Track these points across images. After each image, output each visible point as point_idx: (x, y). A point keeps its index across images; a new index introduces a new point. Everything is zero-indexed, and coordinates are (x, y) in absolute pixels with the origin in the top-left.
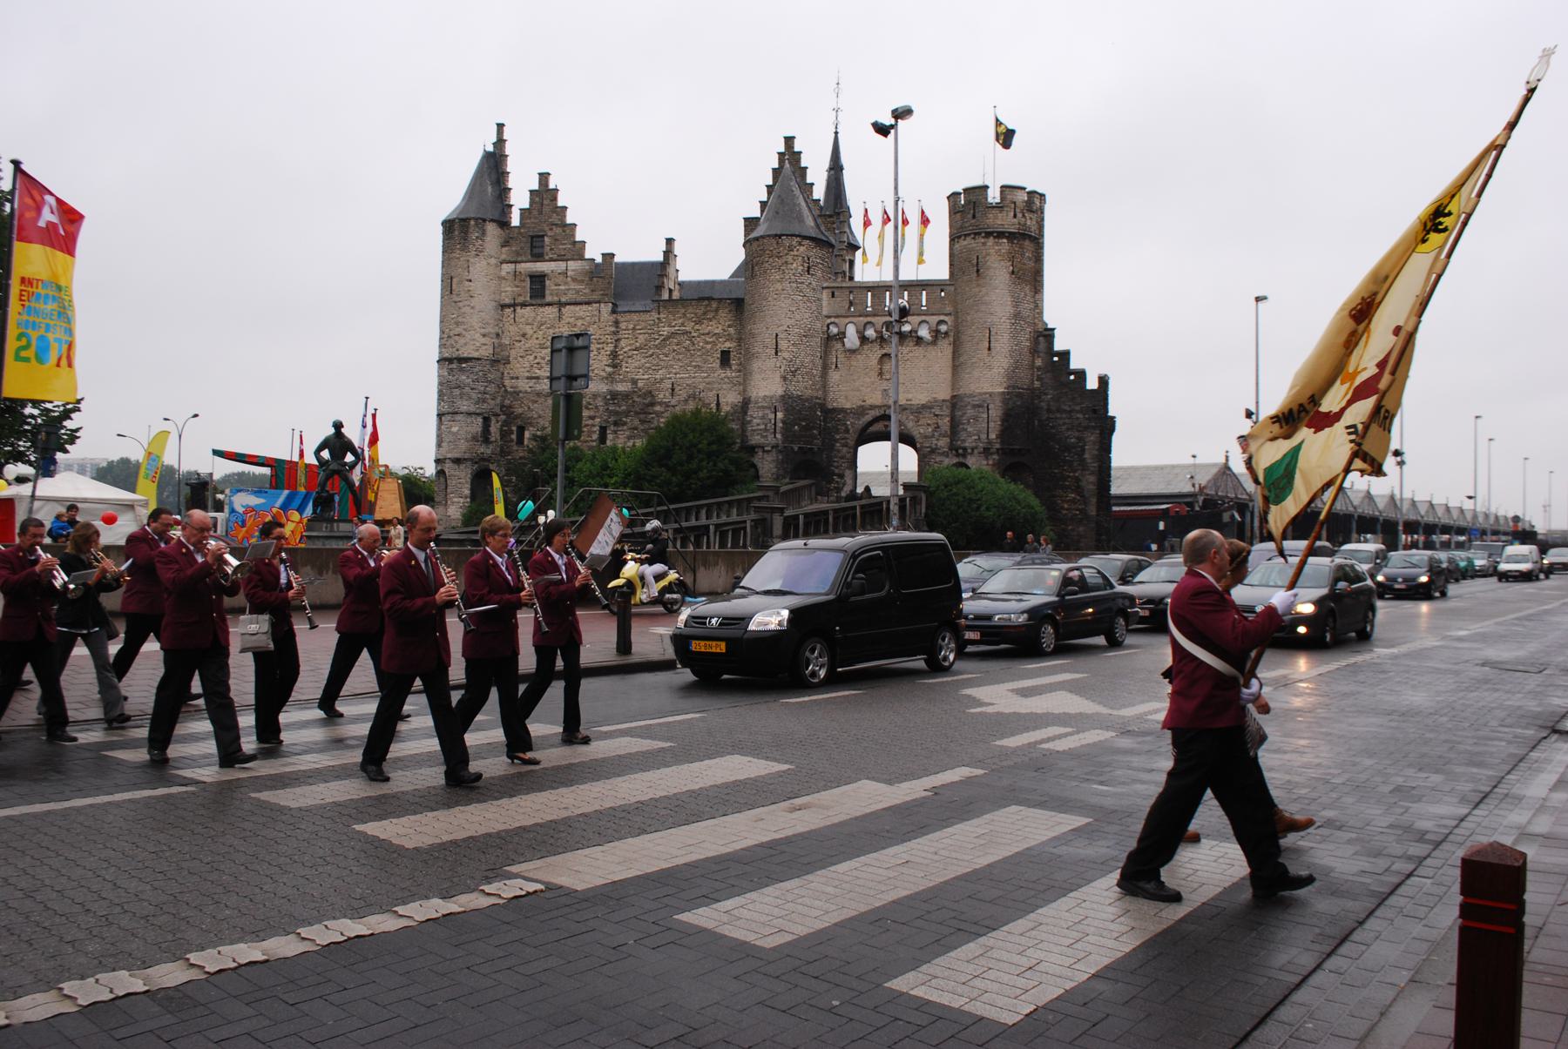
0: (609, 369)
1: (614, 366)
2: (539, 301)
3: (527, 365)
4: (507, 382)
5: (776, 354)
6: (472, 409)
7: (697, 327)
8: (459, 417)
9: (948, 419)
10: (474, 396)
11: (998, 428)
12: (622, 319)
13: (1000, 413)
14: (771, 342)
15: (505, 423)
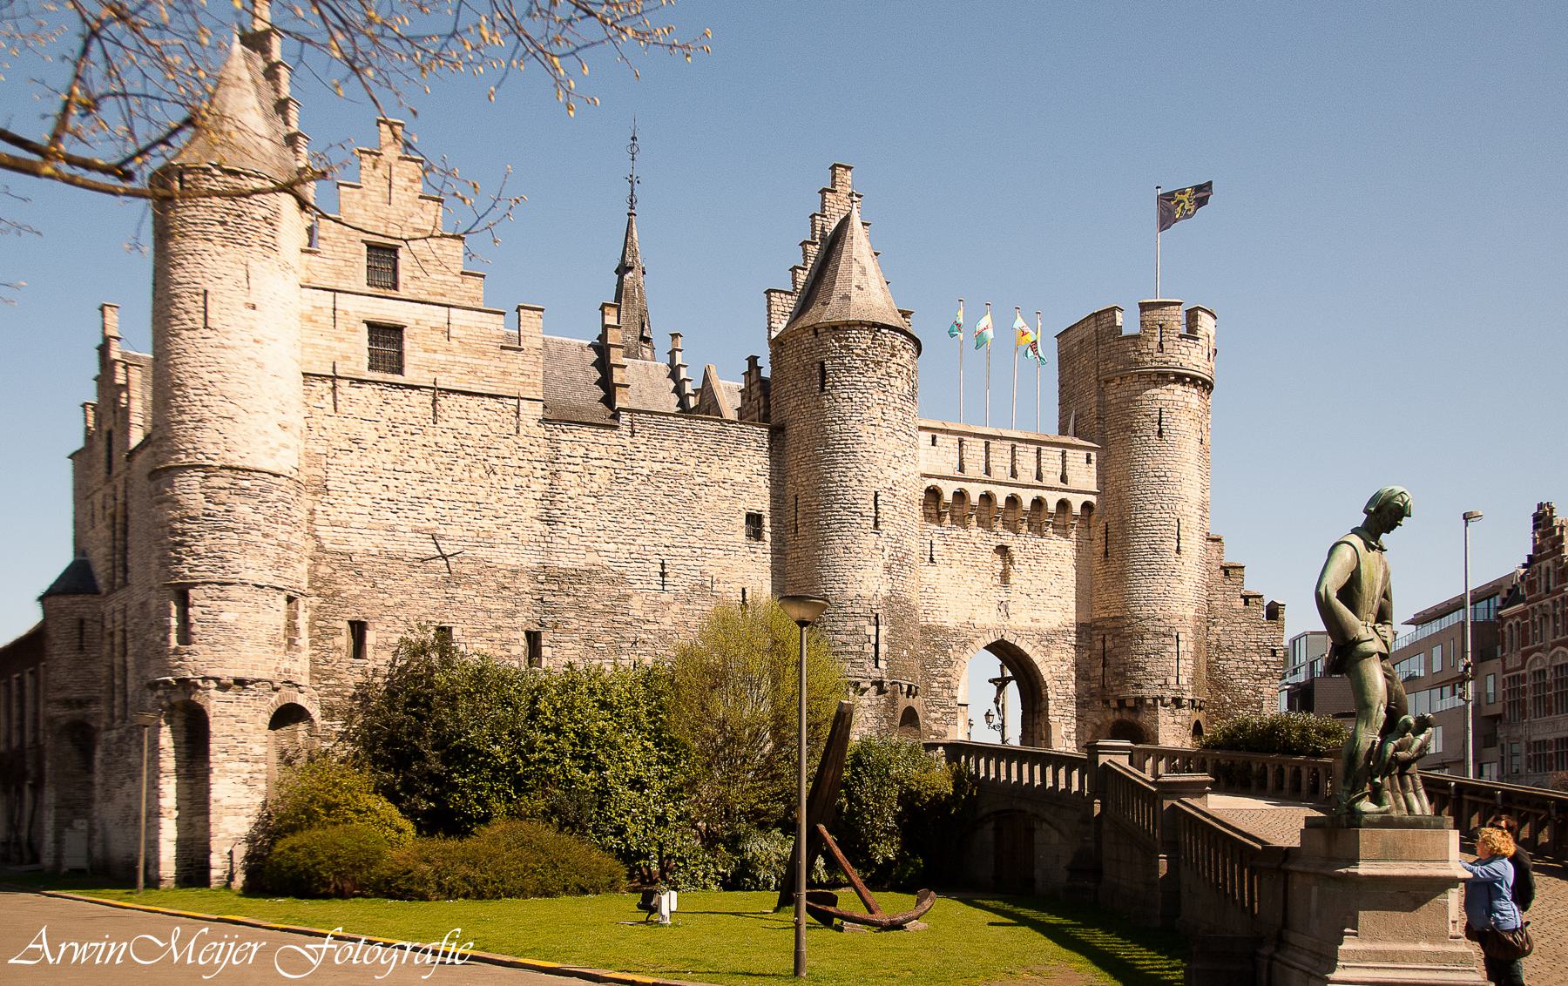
0: (539, 527)
1: (550, 521)
2: (397, 379)
3: (367, 501)
4: (323, 532)
5: (876, 524)
6: (267, 578)
7: (704, 468)
8: (234, 592)
9: (1088, 652)
10: (271, 551)
11: (1190, 669)
12: (563, 436)
13: (1191, 647)
14: (867, 506)
15: (318, 614)
